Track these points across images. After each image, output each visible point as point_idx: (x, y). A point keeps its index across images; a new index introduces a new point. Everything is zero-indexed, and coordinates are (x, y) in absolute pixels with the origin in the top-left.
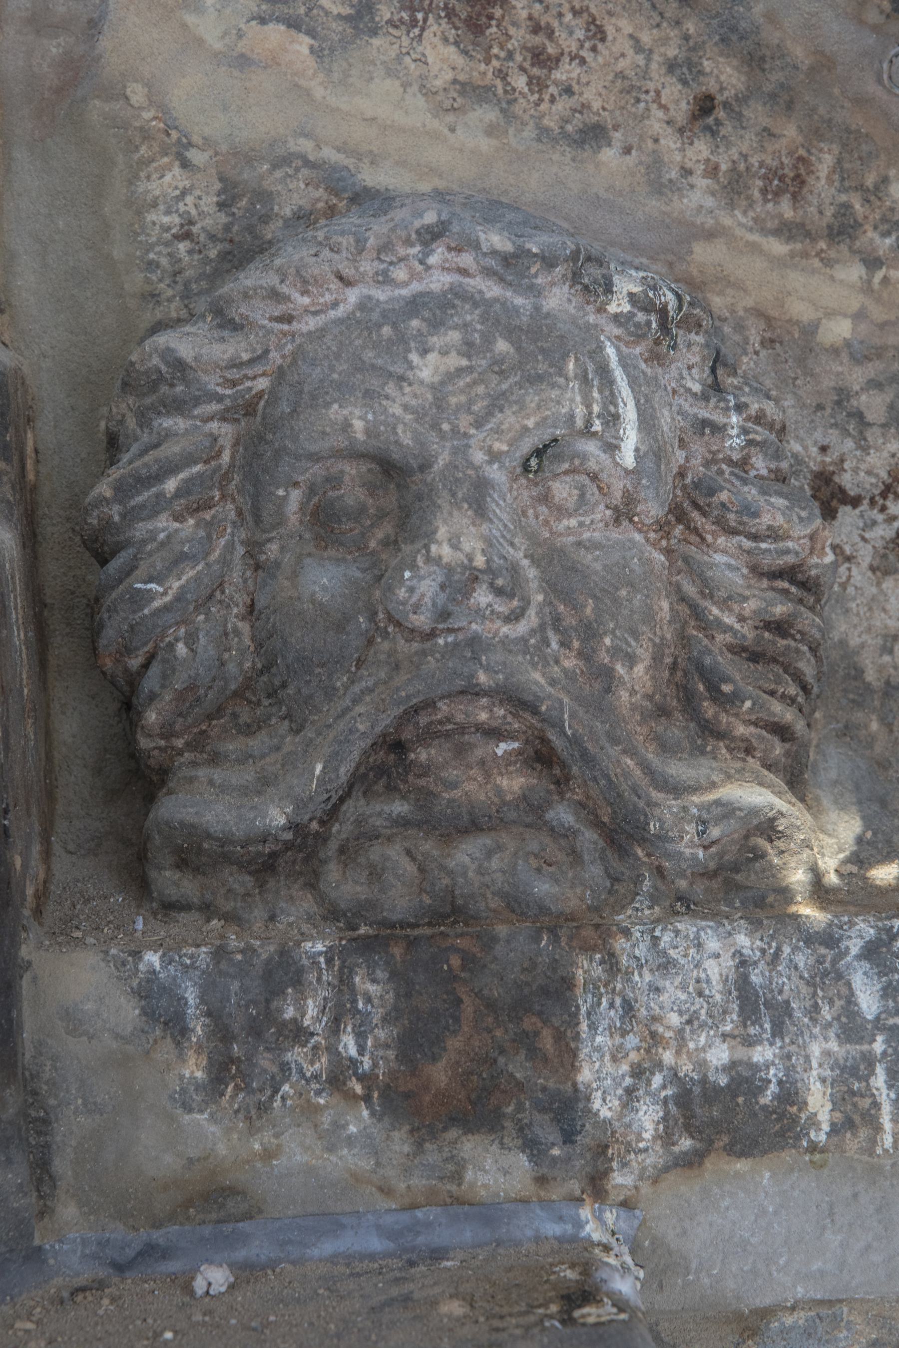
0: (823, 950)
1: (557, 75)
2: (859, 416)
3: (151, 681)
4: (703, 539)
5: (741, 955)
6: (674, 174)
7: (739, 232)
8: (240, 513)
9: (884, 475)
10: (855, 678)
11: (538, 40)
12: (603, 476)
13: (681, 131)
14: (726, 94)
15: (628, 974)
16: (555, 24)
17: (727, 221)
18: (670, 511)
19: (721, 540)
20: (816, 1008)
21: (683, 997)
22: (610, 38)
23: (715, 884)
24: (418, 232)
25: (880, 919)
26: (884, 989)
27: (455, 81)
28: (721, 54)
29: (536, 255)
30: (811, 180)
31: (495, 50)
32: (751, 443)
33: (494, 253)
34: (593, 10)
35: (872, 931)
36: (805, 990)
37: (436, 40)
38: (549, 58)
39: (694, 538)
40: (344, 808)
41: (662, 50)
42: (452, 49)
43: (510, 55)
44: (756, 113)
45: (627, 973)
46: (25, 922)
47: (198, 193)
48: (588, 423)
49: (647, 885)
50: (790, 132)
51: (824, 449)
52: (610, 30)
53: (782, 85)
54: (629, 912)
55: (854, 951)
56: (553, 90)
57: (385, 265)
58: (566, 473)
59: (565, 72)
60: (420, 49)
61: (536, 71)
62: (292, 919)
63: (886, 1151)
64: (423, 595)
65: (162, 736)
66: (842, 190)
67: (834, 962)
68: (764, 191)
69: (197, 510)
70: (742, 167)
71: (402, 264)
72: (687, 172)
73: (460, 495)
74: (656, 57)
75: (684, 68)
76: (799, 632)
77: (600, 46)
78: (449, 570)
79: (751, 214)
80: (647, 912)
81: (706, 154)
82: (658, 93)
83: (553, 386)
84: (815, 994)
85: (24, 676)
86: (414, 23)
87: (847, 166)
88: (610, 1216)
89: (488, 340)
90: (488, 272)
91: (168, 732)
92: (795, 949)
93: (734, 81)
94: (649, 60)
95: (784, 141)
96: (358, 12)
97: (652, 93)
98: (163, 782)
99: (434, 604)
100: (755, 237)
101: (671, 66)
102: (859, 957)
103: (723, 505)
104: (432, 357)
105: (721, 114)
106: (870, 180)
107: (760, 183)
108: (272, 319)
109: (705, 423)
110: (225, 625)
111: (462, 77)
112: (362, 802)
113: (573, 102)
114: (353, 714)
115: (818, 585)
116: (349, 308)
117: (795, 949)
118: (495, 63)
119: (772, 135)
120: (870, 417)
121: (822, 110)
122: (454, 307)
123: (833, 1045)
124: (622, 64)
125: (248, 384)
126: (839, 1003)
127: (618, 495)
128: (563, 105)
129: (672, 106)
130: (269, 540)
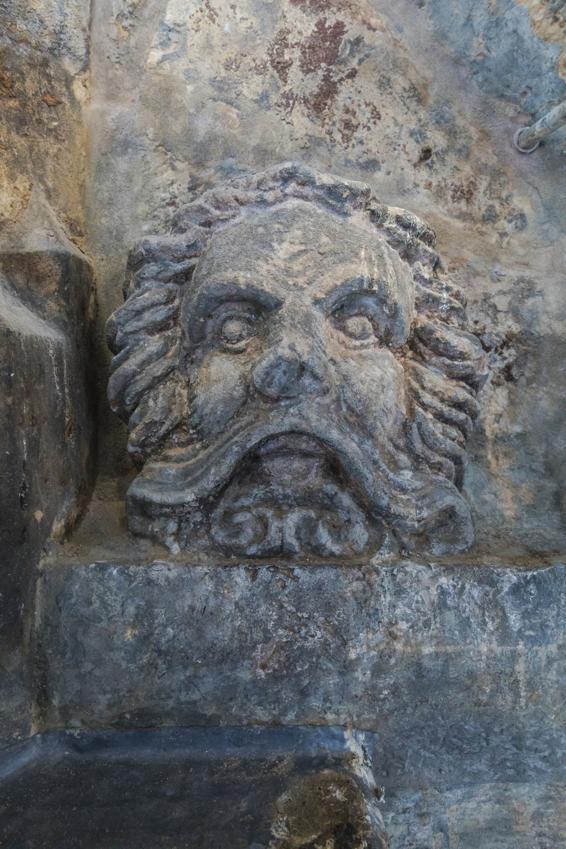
0: (488, 588)
1: (356, 134)
2: (494, 307)
3: (133, 418)
4: (424, 358)
5: (442, 588)
6: (410, 186)
7: (440, 216)
8: (183, 334)
9: (504, 337)
10: (481, 433)
11: (347, 117)
12: (376, 318)
13: (415, 166)
14: (437, 149)
15: (378, 596)
16: (357, 110)
17: (435, 211)
18: (407, 343)
19: (434, 359)
20: (485, 623)
21: (409, 611)
22: (382, 118)
23: (421, 539)
24: (281, 172)
25: (520, 571)
26: (523, 613)
27: (307, 135)
28: (436, 129)
29: (347, 187)
30: (475, 193)
31: (327, 121)
32: (452, 308)
33: (322, 187)
34: (375, 104)
35: (515, 578)
36: (477, 611)
37: (299, 114)
38: (353, 126)
39: (419, 358)
40: (228, 490)
41: (408, 125)
42: (306, 119)
43: (334, 124)
44: (451, 159)
45: (377, 596)
46: (46, 546)
47: (179, 183)
48: (371, 285)
49: (387, 541)
50: (467, 169)
51: (476, 322)
52: (383, 114)
53: (464, 146)
54: (377, 556)
55: (506, 589)
56: (354, 141)
57: (261, 193)
58: (356, 315)
59: (360, 133)
60: (290, 118)
61: (346, 132)
62: (195, 549)
63: (521, 707)
64: (274, 377)
65: (139, 446)
66: (491, 198)
67: (494, 595)
68: (453, 197)
69: (161, 330)
70: (443, 184)
71: (271, 192)
72: (416, 185)
73: (297, 320)
74: (405, 129)
75: (418, 135)
76: (469, 409)
77: (377, 121)
78: (290, 362)
79: (446, 207)
80: (387, 556)
81: (426, 177)
82: (404, 146)
83: (352, 262)
84: (484, 615)
85: (67, 411)
86: (288, 105)
87: (493, 187)
88: (362, 737)
89: (317, 235)
90: (318, 199)
91: (143, 445)
92: (473, 586)
93: (441, 142)
94: (401, 130)
95: (464, 174)
96: (261, 98)
97: (402, 146)
98: (141, 469)
99: (280, 383)
100: (447, 219)
101: (412, 134)
102: (507, 594)
103: (437, 339)
104: (285, 245)
105: (435, 159)
106: (504, 196)
107: (451, 193)
108: (200, 225)
109: (429, 295)
110: (174, 392)
111: (310, 133)
112: (237, 487)
113: (363, 148)
114: (233, 441)
115: (477, 386)
116: (242, 218)
117: (473, 586)
118: (327, 127)
119: (458, 170)
120: (500, 308)
121: (483, 160)
122: (299, 216)
123: (494, 645)
124: (388, 131)
125: (187, 261)
126: (498, 621)
127: (383, 330)
128: (359, 149)
129: (411, 153)
130: (197, 347)
